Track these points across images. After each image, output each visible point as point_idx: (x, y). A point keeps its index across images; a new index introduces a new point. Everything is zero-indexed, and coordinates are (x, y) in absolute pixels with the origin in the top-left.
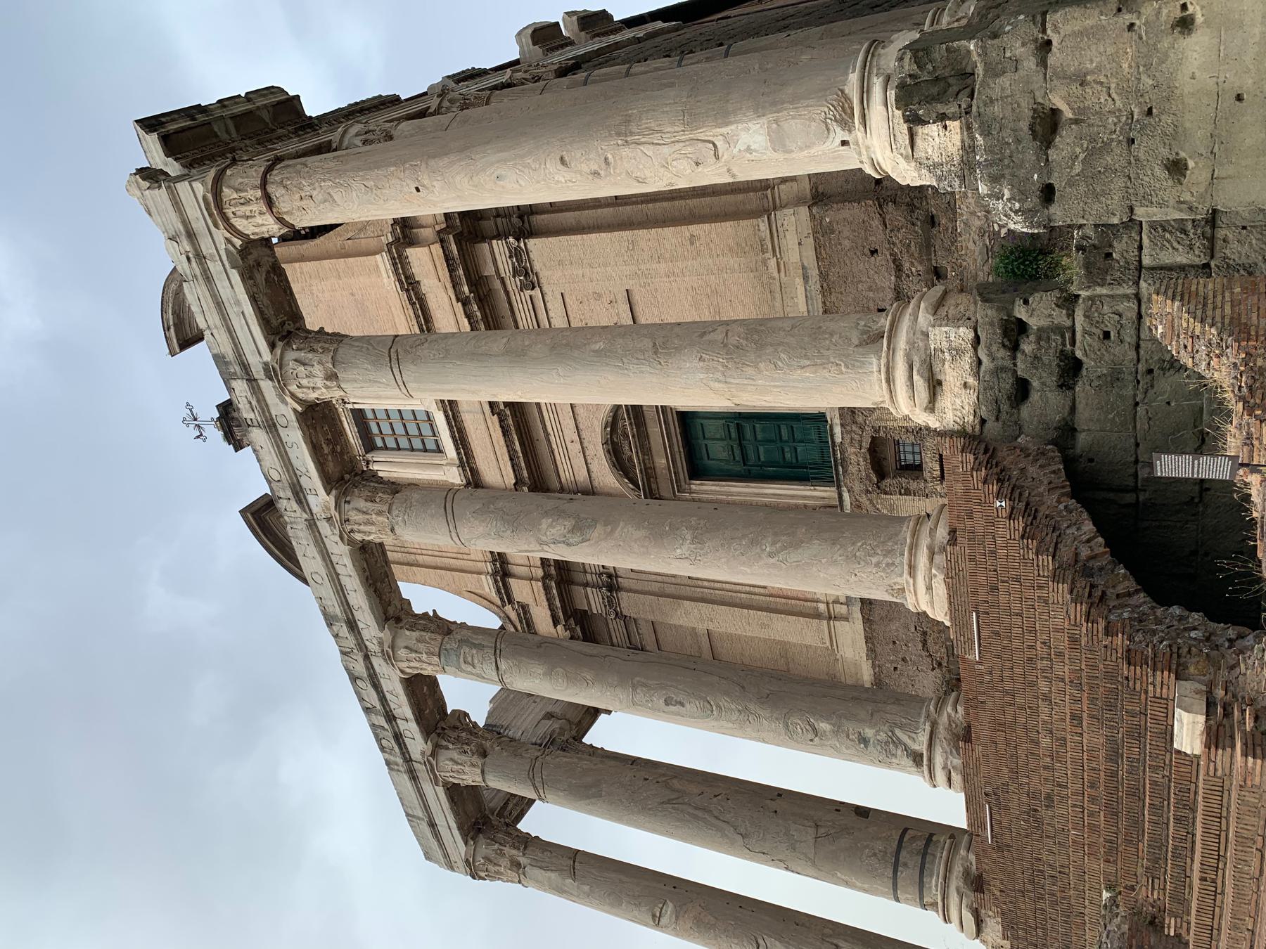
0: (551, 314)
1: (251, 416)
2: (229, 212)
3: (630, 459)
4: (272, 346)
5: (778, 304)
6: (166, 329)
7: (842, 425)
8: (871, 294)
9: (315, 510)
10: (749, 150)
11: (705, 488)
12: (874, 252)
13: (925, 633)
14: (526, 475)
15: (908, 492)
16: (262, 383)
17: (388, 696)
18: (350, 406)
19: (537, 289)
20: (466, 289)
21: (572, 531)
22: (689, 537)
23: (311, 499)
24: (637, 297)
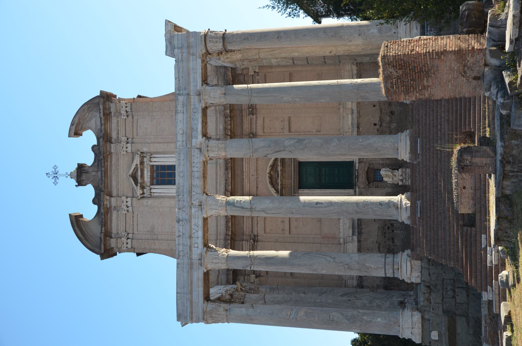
0: (258, 124)
1: (182, 109)
2: (208, 41)
3: (276, 181)
4: (202, 85)
5: (341, 123)
6: (72, 124)
7: (359, 163)
8: (372, 119)
9: (193, 144)
10: (373, 33)
11: (304, 192)
12: (374, 106)
13: (379, 244)
14: (230, 188)
15: (377, 187)
16: (192, 97)
17: (193, 226)
18: (152, 164)
19: (255, 116)
20: (228, 111)
21: (297, 142)
22: (336, 141)
23: (194, 141)
24: (292, 119)
